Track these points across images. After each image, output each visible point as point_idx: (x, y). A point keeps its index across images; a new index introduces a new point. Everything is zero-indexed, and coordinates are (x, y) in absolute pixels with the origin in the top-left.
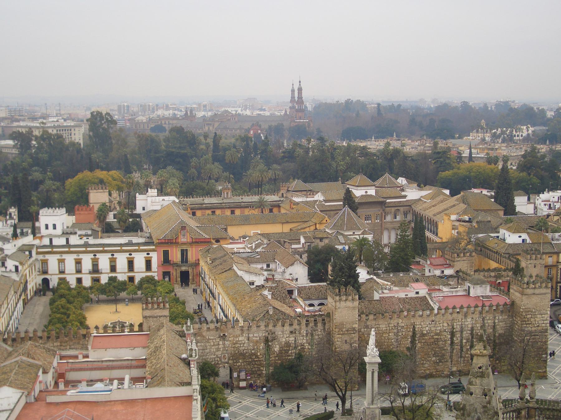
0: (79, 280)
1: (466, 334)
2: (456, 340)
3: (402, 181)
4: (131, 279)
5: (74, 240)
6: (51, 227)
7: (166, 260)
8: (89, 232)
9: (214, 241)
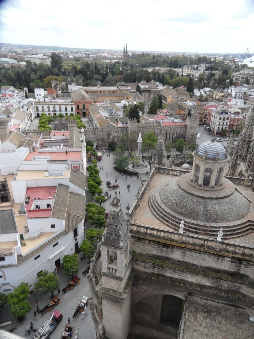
0: (49, 114)
1: (171, 134)
2: (168, 136)
3: (157, 83)
4: (67, 114)
5: (47, 100)
6: (39, 95)
7: (78, 107)
8: (52, 97)
9: (93, 102)
